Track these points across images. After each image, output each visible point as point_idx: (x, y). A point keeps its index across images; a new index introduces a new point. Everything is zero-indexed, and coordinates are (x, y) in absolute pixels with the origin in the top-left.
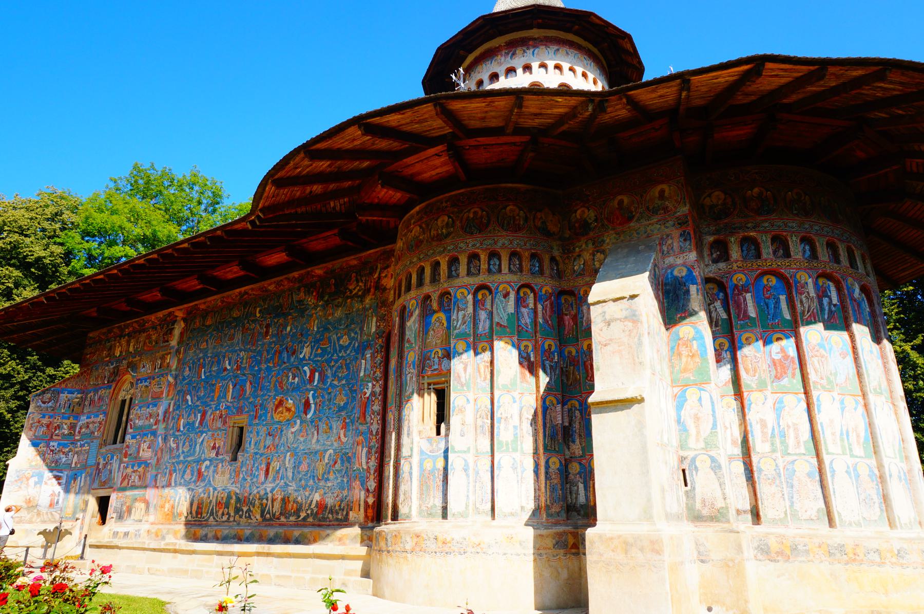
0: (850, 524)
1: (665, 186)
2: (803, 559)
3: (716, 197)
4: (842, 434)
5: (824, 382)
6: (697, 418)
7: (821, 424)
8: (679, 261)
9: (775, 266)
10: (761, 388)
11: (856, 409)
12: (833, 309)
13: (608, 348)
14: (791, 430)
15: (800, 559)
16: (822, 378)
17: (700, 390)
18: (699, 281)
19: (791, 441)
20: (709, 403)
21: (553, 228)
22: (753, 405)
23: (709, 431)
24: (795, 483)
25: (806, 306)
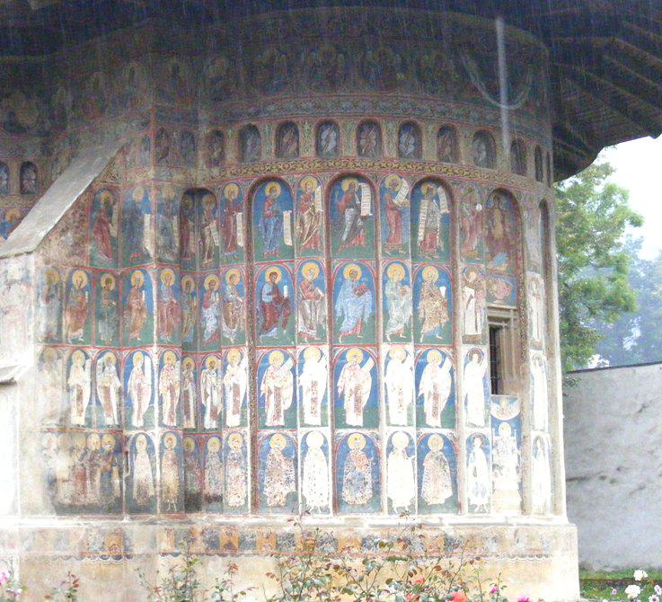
0: (315, 511)
1: (133, 64)
2: (250, 552)
3: (215, 67)
4: (325, 399)
5: (313, 333)
6: (140, 390)
7: (301, 387)
8: (139, 179)
9: (275, 171)
10: (239, 342)
11: (362, 365)
12: (360, 223)
13: (8, 317)
14: (272, 397)
15: (246, 552)
16: (311, 328)
17: (145, 354)
18: (154, 208)
19: (270, 411)
20: (150, 371)
21: (26, 119)
22: (229, 367)
23: (147, 406)
24: (269, 462)
25: (307, 226)
